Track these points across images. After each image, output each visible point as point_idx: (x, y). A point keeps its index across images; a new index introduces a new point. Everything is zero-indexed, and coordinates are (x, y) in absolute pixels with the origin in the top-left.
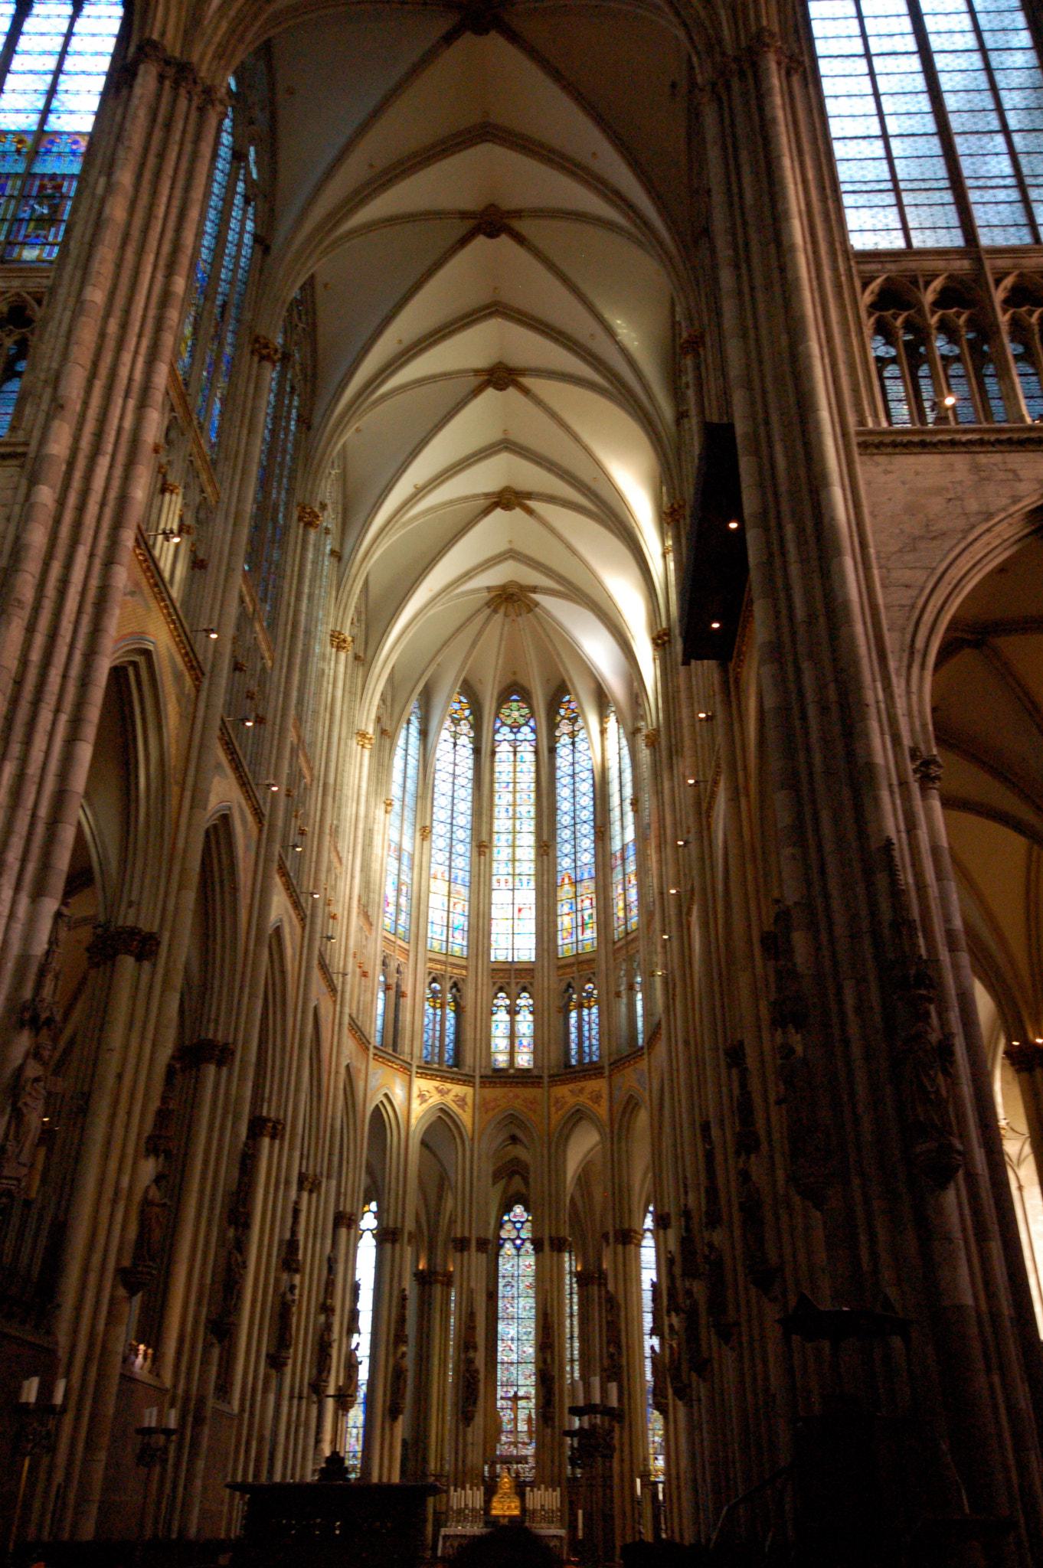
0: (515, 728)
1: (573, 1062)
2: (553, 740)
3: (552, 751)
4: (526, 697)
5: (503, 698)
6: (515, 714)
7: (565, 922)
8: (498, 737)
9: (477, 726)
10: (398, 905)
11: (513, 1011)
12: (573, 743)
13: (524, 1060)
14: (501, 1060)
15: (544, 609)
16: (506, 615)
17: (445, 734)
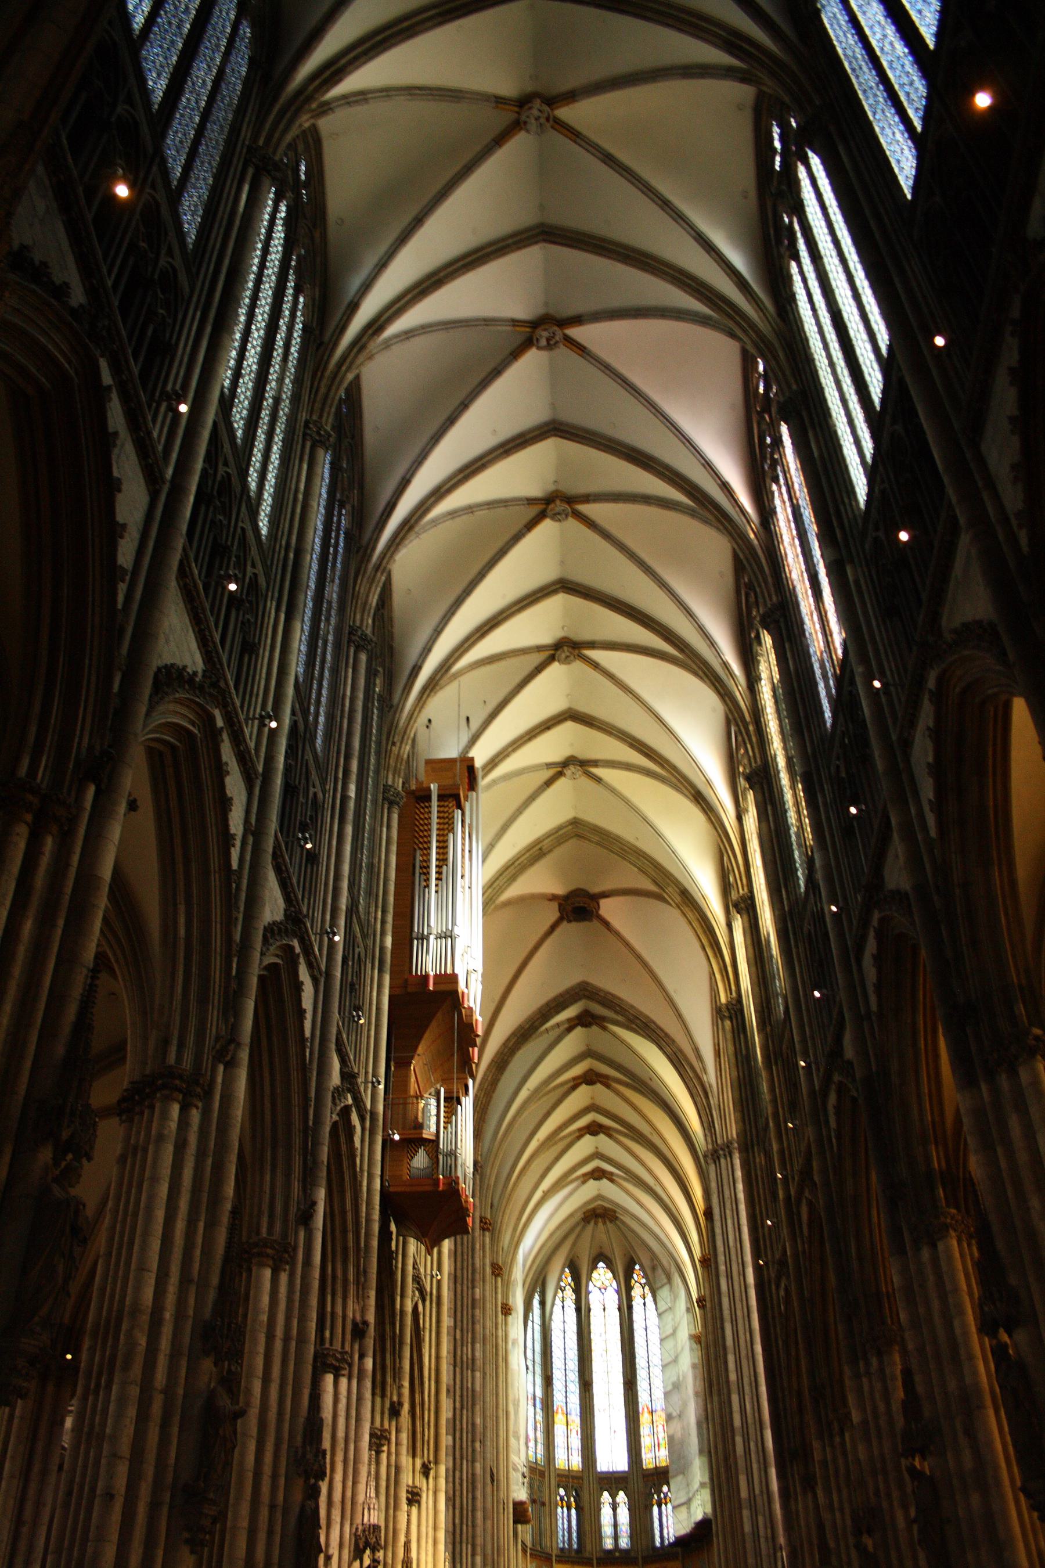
0: (602, 1289)
1: (658, 1543)
2: (630, 1299)
3: (630, 1307)
4: (610, 1266)
5: (595, 1267)
6: (603, 1278)
7: (646, 1441)
8: (591, 1296)
9: (577, 1290)
10: (536, 1441)
11: (614, 1507)
12: (644, 1304)
13: (624, 1542)
14: (608, 1544)
15: (623, 1223)
16: (596, 1223)
17: (558, 1302)
